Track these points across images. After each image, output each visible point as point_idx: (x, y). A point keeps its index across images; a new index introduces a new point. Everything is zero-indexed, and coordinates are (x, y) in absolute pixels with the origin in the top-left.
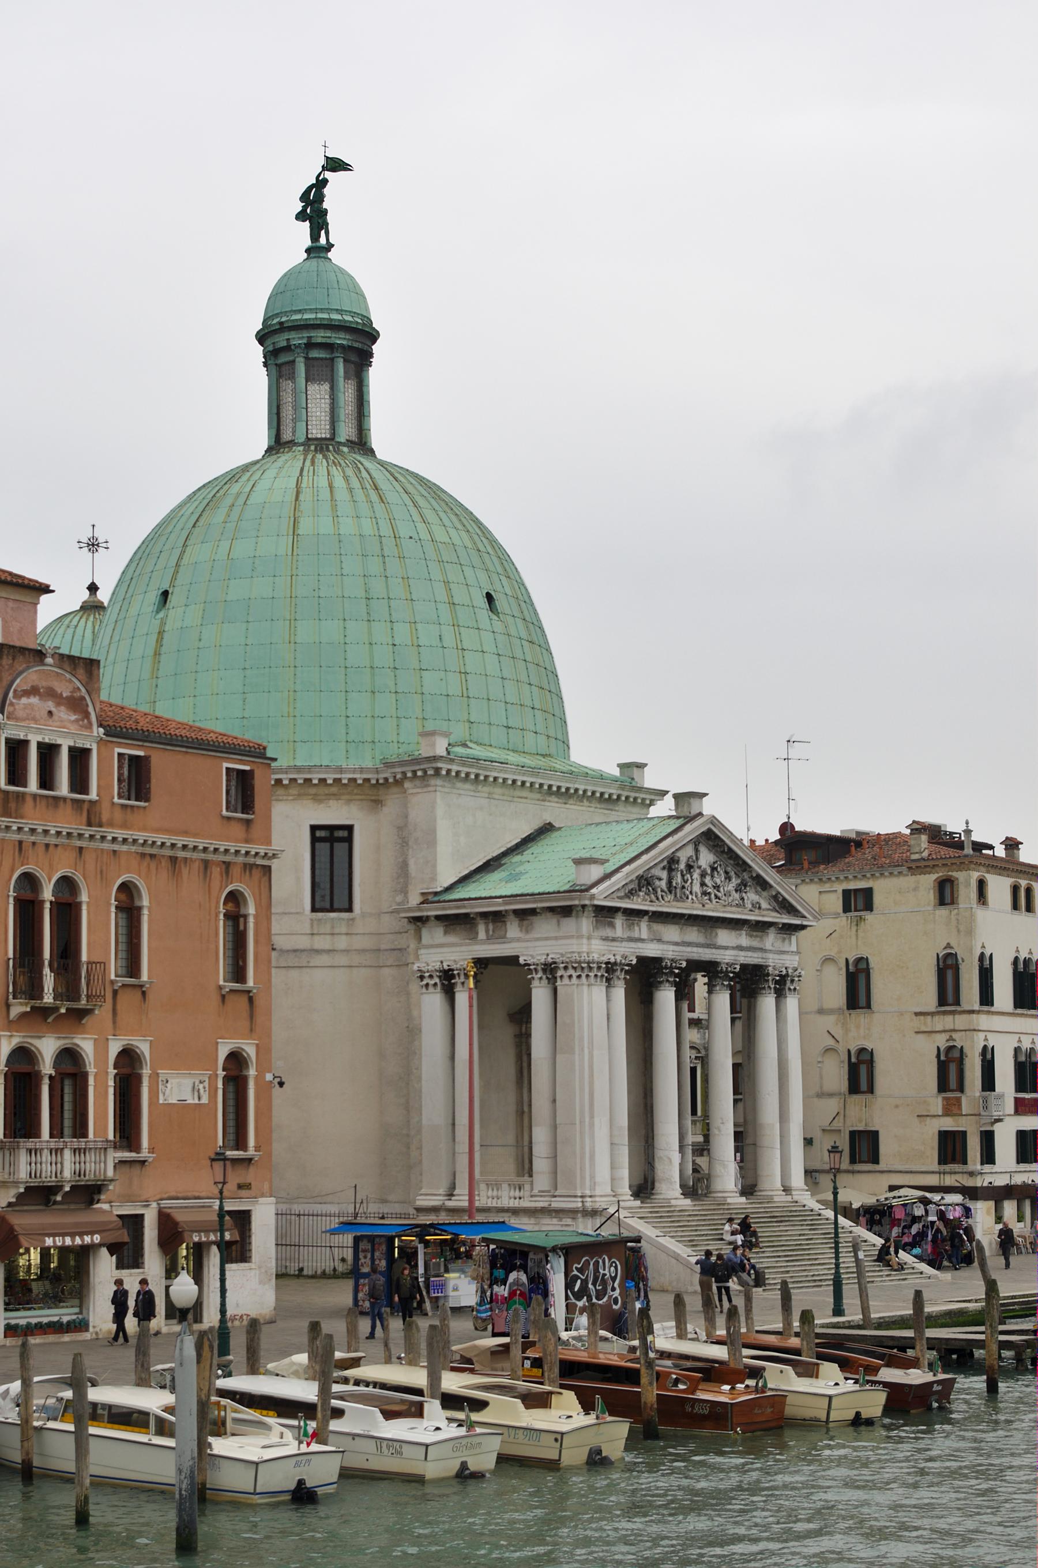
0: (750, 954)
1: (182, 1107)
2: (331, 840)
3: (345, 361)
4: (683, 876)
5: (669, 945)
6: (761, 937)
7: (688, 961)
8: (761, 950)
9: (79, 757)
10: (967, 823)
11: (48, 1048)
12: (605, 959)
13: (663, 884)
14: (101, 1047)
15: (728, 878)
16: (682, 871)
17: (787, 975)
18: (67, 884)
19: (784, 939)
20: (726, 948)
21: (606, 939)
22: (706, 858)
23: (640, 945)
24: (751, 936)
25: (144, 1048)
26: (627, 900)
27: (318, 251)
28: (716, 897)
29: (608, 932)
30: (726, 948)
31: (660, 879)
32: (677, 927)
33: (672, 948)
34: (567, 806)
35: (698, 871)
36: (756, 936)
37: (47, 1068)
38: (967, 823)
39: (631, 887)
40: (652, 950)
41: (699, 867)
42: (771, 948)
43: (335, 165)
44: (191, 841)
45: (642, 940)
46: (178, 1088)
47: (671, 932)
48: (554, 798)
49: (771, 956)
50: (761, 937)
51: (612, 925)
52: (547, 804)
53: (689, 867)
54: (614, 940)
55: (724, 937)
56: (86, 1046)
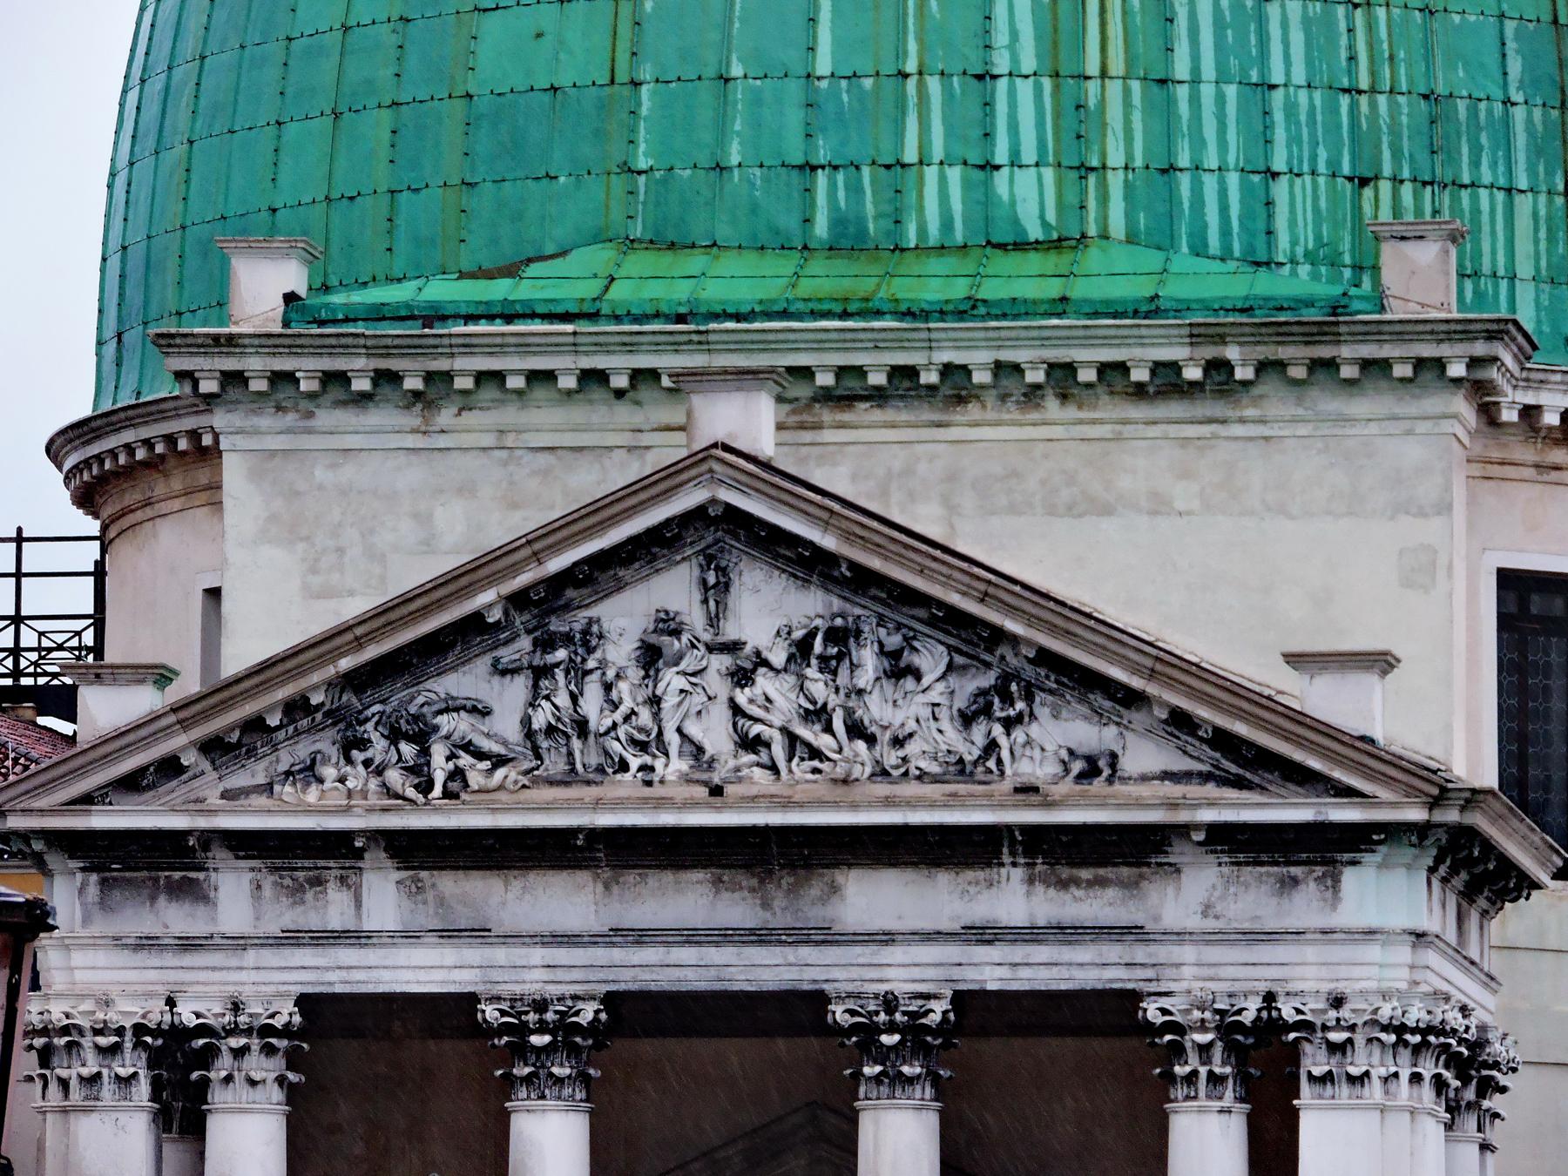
0: (1042, 953)
4: (608, 687)
5: (537, 947)
7: (611, 1000)
8: (1133, 932)
12: (127, 1012)
13: (506, 725)
15: (898, 669)
16: (603, 665)
17: (1270, 1027)
20: (887, 938)
21: (147, 944)
22: (766, 608)
23: (347, 955)
24: (1063, 885)
26: (261, 801)
28: (815, 753)
29: (176, 918)
30: (887, 938)
31: (481, 711)
32: (583, 877)
33: (538, 955)
34: (954, 433)
35: (721, 662)
36: (1101, 882)
39: (303, 750)
41: (733, 647)
42: (1194, 922)
48: (863, 412)
49: (1188, 953)
50: (1132, 885)
51: (193, 892)
52: (828, 435)
53: (650, 657)
54: (188, 945)
55: (869, 896)
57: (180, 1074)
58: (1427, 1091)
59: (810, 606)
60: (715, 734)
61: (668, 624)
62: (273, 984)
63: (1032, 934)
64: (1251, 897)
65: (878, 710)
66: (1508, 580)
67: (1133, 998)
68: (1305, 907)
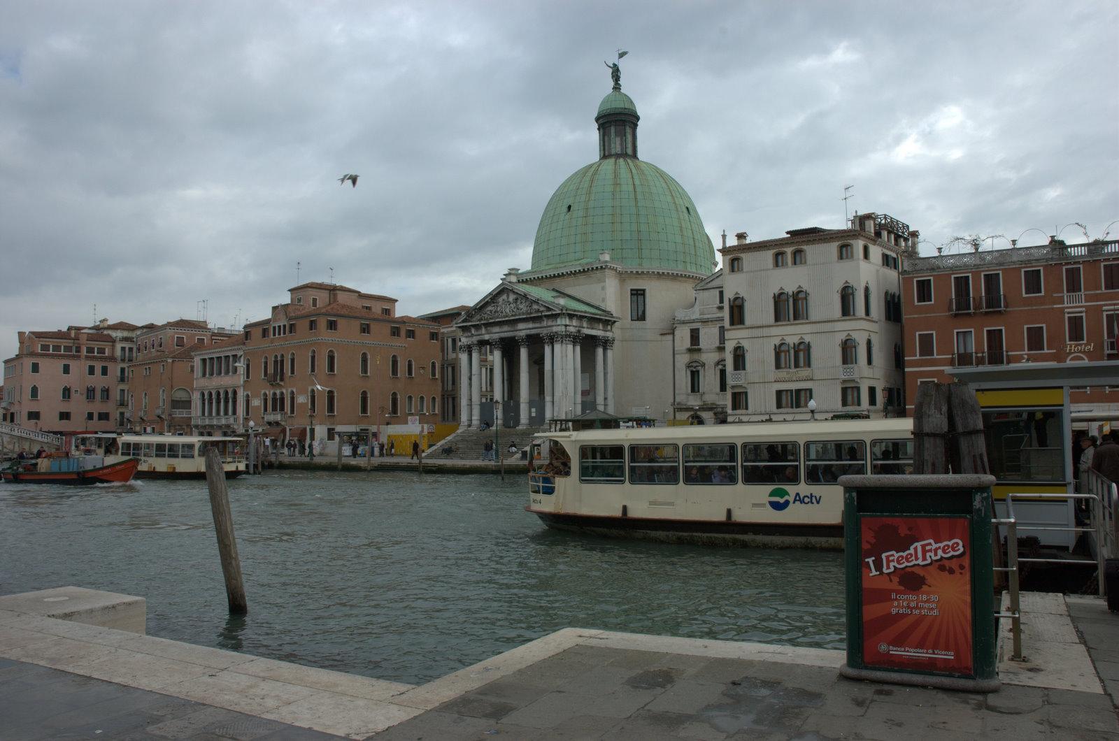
1: (302, 404)
2: (637, 295)
3: (604, 129)
6: (540, 323)
9: (285, 326)
10: (724, 231)
11: (278, 392)
14: (287, 390)
17: (550, 336)
18: (282, 356)
19: (553, 321)
20: (521, 330)
21: (466, 337)
25: (295, 390)
27: (617, 87)
30: (521, 330)
37: (278, 397)
38: (724, 231)
40: (487, 337)
43: (622, 55)
44: (301, 340)
45: (482, 335)
46: (301, 399)
47: (496, 329)
55: (521, 326)
56: (284, 391)
57: (469, 349)
58: (569, 342)
59: (515, 296)
60: (508, 310)
61: (503, 300)
62: (475, 339)
63: (533, 329)
64: (550, 323)
65: (521, 306)
66: (632, 290)
67: (539, 334)
68: (554, 323)
